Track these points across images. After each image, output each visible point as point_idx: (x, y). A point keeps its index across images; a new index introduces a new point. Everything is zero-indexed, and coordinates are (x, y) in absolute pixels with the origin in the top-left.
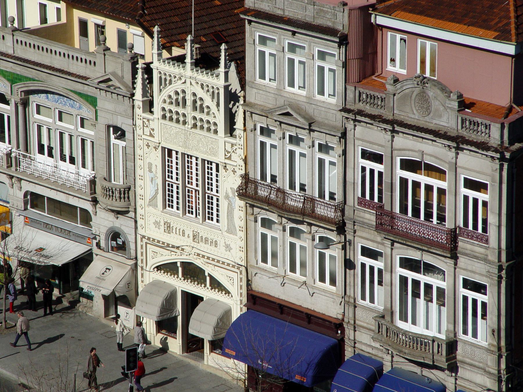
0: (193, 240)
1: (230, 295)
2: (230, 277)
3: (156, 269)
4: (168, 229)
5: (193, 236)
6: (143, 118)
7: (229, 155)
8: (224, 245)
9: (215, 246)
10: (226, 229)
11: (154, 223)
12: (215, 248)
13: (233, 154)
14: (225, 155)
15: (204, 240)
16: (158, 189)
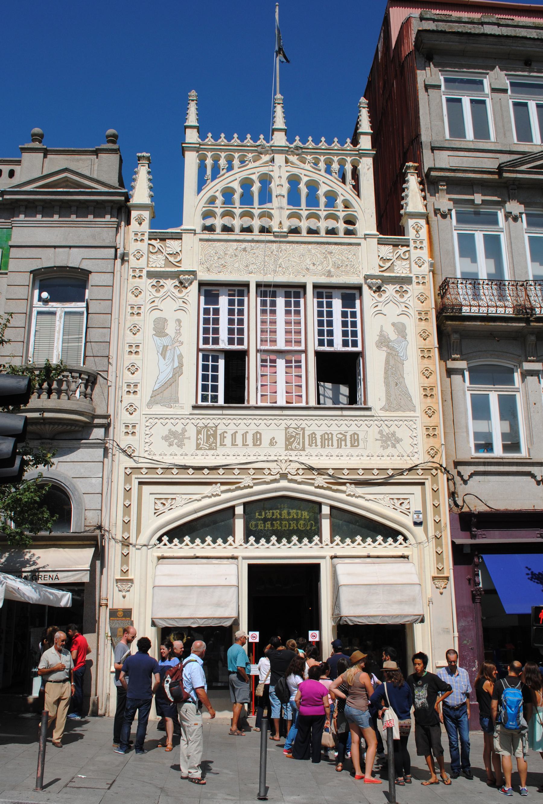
0: (286, 446)
1: (400, 538)
2: (398, 499)
3: (165, 539)
4: (208, 439)
5: (287, 439)
6: (150, 239)
7: (388, 265)
8: (378, 436)
9: (352, 446)
10: (383, 403)
11: (165, 438)
12: (354, 451)
13: (398, 263)
14: (381, 267)
15: (319, 441)
16: (181, 365)
